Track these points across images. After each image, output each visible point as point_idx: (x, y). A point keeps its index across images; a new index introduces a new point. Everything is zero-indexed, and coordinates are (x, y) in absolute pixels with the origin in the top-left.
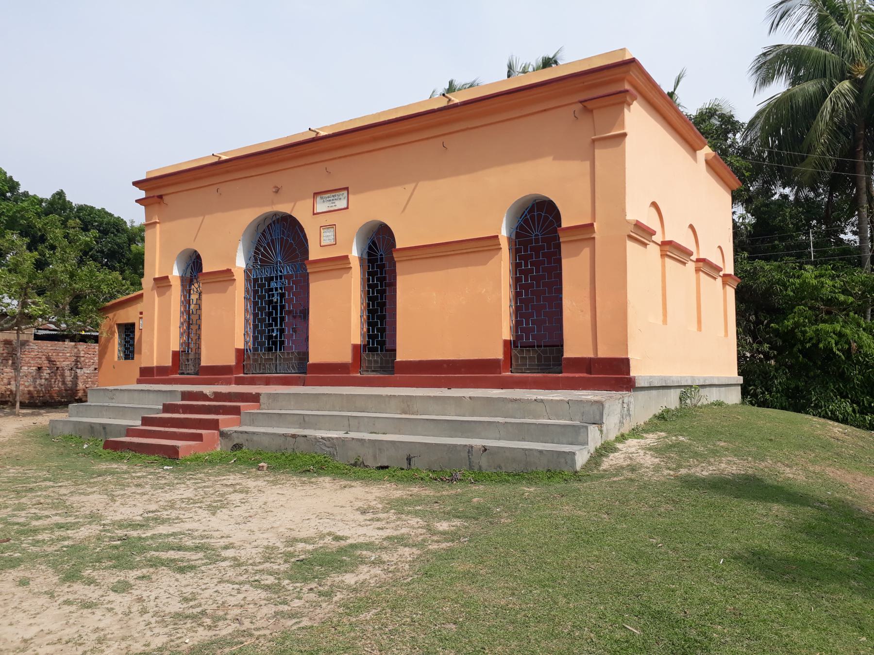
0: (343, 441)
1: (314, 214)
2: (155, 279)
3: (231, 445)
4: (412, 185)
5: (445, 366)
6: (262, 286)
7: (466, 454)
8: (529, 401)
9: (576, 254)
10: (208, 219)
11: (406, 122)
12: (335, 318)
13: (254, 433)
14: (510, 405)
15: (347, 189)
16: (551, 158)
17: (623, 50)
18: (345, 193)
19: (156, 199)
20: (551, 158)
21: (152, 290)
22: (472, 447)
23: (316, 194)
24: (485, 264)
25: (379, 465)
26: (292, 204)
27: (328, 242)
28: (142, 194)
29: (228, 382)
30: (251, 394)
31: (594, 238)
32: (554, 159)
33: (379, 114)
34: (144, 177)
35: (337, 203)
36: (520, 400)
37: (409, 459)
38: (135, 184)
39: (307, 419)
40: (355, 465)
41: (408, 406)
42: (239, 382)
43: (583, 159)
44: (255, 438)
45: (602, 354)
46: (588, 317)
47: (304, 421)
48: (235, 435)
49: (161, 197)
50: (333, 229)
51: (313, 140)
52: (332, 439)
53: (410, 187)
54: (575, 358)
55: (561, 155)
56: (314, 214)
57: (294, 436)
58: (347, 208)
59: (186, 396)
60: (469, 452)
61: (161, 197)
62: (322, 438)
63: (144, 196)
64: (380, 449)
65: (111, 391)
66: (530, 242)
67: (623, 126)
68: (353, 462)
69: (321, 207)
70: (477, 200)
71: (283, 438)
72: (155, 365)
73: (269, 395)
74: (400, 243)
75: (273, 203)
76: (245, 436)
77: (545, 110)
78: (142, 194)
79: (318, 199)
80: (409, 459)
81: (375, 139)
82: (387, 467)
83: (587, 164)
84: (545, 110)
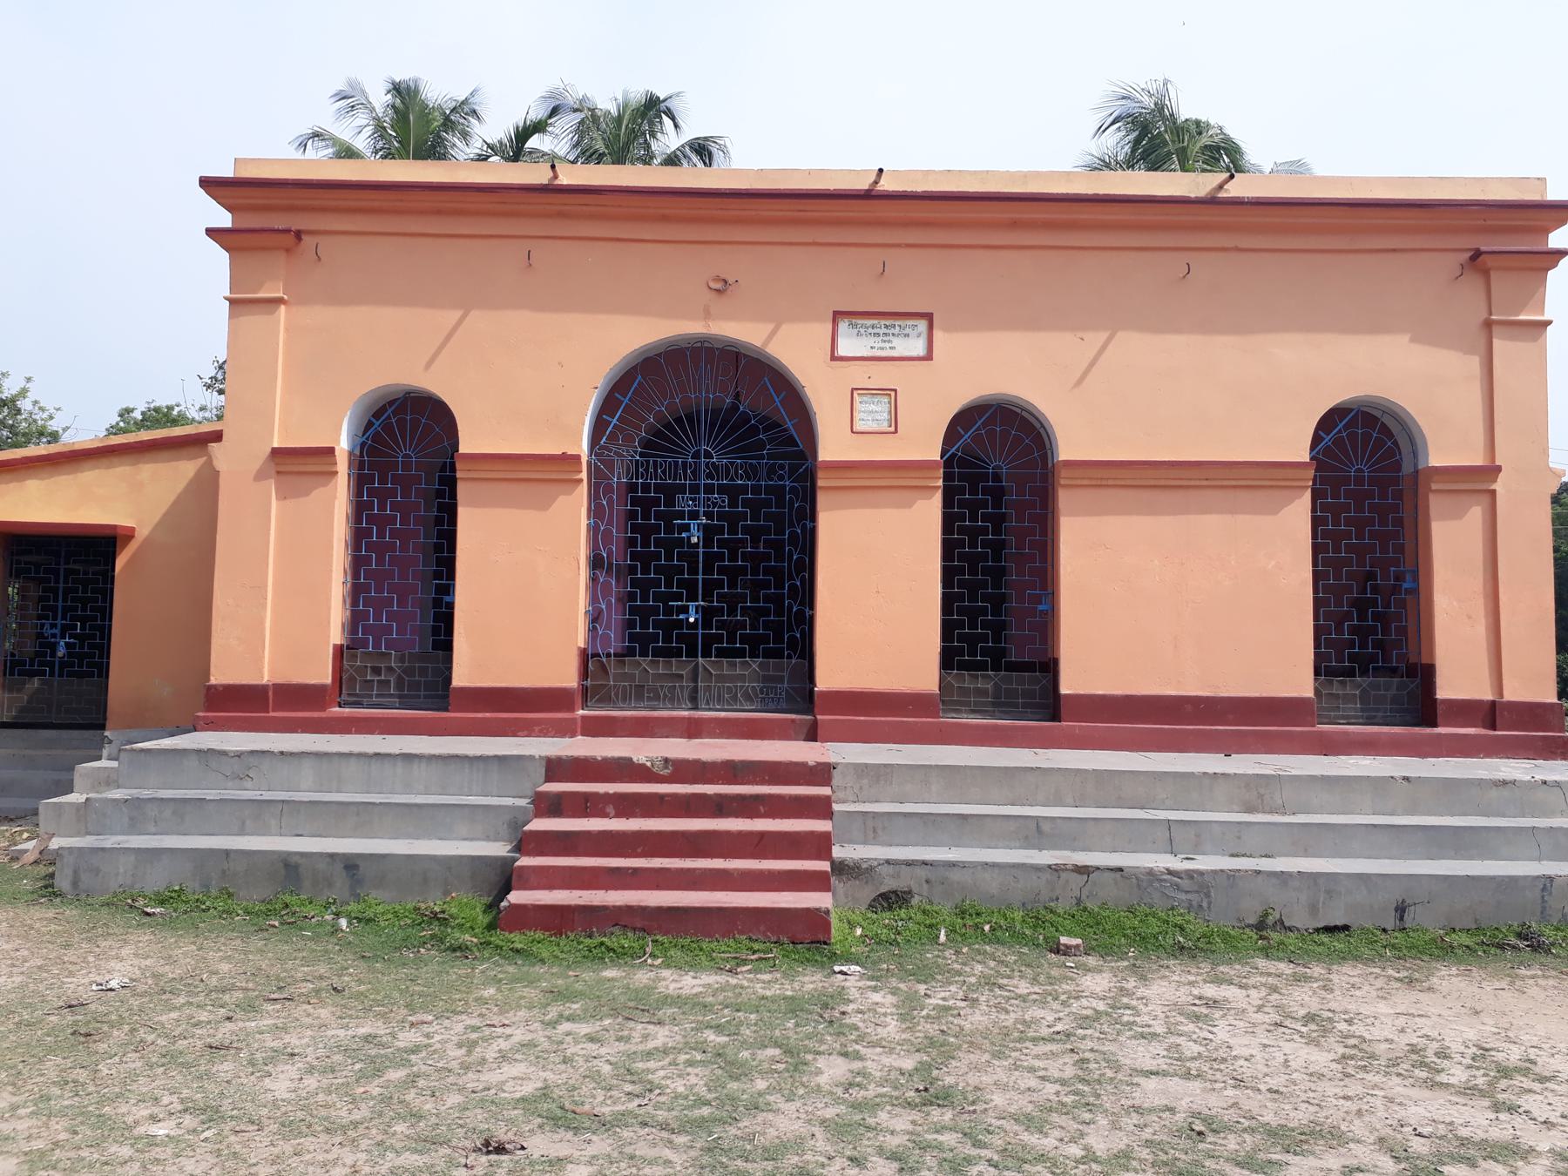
0: (1232, 875)
1: (834, 358)
2: (276, 452)
3: (868, 893)
4: (1104, 336)
5: (1189, 708)
6: (647, 504)
7: (1538, 893)
8: (1480, 783)
9: (1458, 514)
10: (481, 321)
11: (1116, 207)
12: (877, 591)
13: (952, 865)
14: (1494, 793)
15: (929, 317)
16: (1406, 338)
17: (1542, 180)
18: (922, 325)
19: (291, 238)
20: (1406, 338)
21: (260, 476)
22: (1551, 879)
23: (837, 316)
24: (1460, 518)
25: (1321, 925)
26: (771, 327)
27: (873, 426)
28: (224, 219)
29: (565, 730)
30: (804, 765)
31: (1493, 492)
32: (1412, 340)
33: (1051, 175)
34: (228, 172)
35: (896, 342)
36: (1514, 782)
37: (1401, 910)
38: (208, 184)
39: (1046, 827)
40: (1260, 926)
41: (1261, 796)
42: (595, 728)
43: (1470, 351)
44: (955, 876)
45: (1510, 695)
46: (1481, 629)
47: (1036, 833)
48: (885, 869)
49: (298, 235)
50: (877, 398)
51: (869, 195)
52: (1201, 873)
53: (1096, 338)
54: (1463, 701)
55: (1426, 335)
56: (834, 358)
57: (1055, 869)
58: (929, 357)
59: (555, 768)
60: (1544, 889)
61: (298, 235)
62: (1170, 872)
63: (229, 225)
64: (1328, 892)
65: (239, 755)
66: (1347, 480)
67: (1541, 308)
68: (1252, 920)
69: (849, 344)
70: (1264, 387)
71: (1047, 876)
72: (266, 678)
73: (862, 770)
74: (1067, 449)
75: (707, 315)
76: (922, 873)
77: (1394, 250)
78: (224, 219)
79: (843, 326)
80: (1401, 910)
81: (1014, 225)
82: (1346, 928)
83: (1474, 363)
84: (1394, 250)
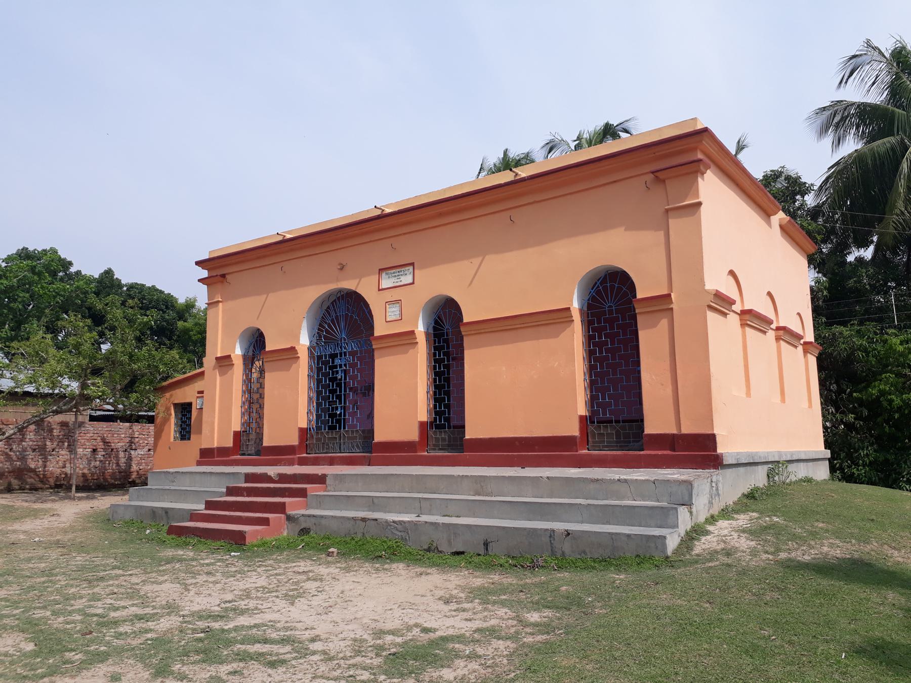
0: (415, 524)
1: (379, 290)
2: (217, 358)
3: (298, 529)
4: (480, 259)
5: (517, 443)
6: (325, 363)
7: (548, 539)
8: (612, 481)
9: (654, 325)
10: (272, 296)
12: (401, 395)
13: (322, 517)
14: (592, 486)
15: (412, 264)
17: (695, 119)
18: (411, 268)
22: (553, 531)
23: (381, 270)
27: (393, 318)
28: (204, 274)
29: (291, 463)
30: (317, 475)
31: (672, 309)
32: (625, 230)
33: (445, 190)
34: (206, 256)
35: (403, 278)
36: (602, 480)
37: (486, 544)
38: (198, 263)
39: (376, 501)
40: (429, 550)
41: (482, 487)
42: (302, 462)
44: (323, 522)
45: (685, 430)
46: (669, 391)
47: (373, 503)
48: (302, 519)
50: (398, 304)
53: (476, 261)
56: (379, 290)
57: (364, 520)
59: (249, 478)
60: (550, 536)
61: (223, 276)
62: (394, 522)
64: (455, 534)
65: (173, 473)
67: (697, 195)
68: (426, 547)
69: (386, 282)
70: (548, 272)
71: (352, 522)
72: (215, 445)
75: (338, 280)
76: (313, 520)
78: (204, 274)
79: (384, 275)
80: (486, 544)
81: (441, 215)
82: (463, 553)
83: (661, 234)
